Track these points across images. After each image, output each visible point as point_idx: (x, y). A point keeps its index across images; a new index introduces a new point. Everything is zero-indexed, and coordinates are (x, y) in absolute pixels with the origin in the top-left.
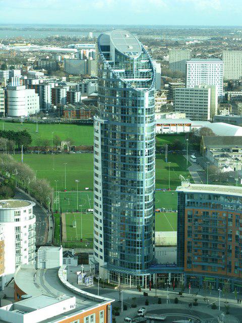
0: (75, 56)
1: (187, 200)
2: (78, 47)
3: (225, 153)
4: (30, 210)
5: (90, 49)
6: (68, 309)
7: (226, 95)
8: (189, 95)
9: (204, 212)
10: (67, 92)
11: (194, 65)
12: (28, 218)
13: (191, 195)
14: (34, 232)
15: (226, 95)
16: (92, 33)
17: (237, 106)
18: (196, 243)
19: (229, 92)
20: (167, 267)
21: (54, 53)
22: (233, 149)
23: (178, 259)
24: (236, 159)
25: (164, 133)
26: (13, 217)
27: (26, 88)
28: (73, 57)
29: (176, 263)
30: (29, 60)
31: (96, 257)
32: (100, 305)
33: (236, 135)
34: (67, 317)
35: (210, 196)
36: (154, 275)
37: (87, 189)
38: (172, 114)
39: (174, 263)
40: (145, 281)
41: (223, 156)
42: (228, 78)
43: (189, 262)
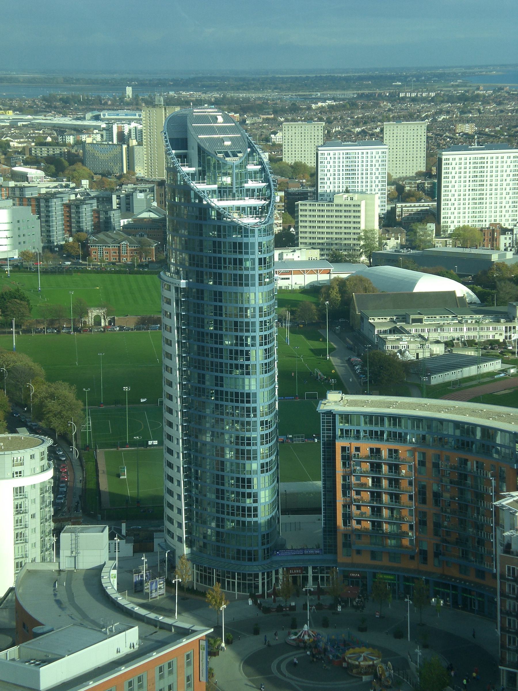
0: (102, 136)
1: (340, 426)
2: (107, 117)
3: (399, 325)
4: (42, 453)
5: (129, 121)
6: (126, 650)
7: (393, 210)
8: (325, 213)
9: (372, 450)
10: (93, 211)
11: (332, 155)
12: (38, 470)
13: (346, 417)
14: (50, 497)
15: (393, 210)
16: (131, 88)
17: (415, 233)
18: (358, 507)
19: (399, 205)
20: (304, 554)
21: (61, 130)
22: (412, 317)
23: (325, 538)
24: (421, 336)
25: (280, 287)
26: (10, 470)
27: (14, 205)
28: (98, 138)
29: (322, 547)
30: (11, 143)
31: (168, 538)
32: (185, 641)
33: (417, 289)
34: (124, 670)
35: (379, 419)
36: (281, 571)
37: (142, 400)
38: (294, 251)
39: (318, 547)
40: (263, 584)
41: (394, 331)
42: (395, 176)
43: (347, 545)
